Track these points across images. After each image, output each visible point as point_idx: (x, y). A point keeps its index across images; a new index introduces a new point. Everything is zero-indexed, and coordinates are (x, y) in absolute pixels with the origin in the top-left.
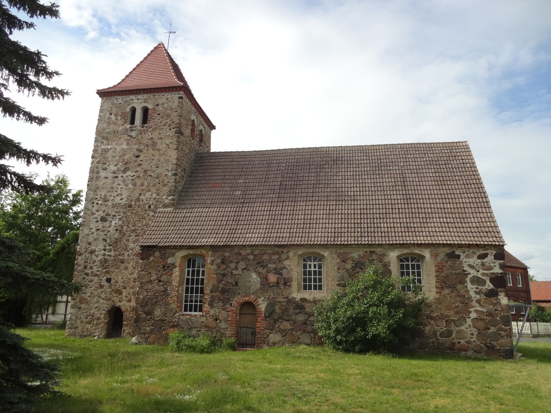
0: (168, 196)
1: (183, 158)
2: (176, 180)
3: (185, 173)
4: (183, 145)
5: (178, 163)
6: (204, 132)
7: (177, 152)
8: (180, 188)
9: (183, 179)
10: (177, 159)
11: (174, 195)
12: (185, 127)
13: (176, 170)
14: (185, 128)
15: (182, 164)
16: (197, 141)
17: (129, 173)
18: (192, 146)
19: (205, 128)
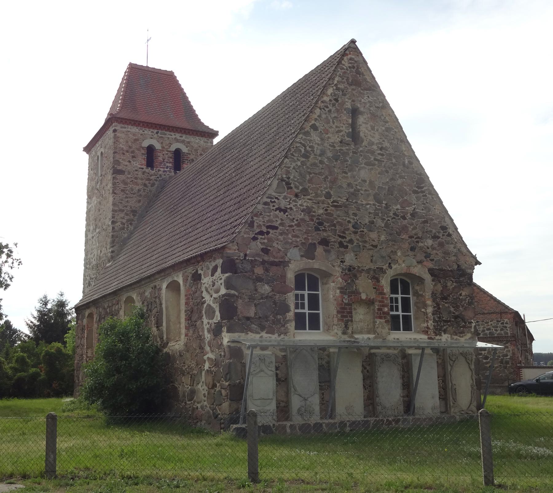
0: (110, 249)
1: (126, 200)
2: (113, 228)
3: (134, 215)
4: (125, 183)
5: (116, 208)
6: (185, 149)
7: (113, 197)
8: (126, 235)
9: (131, 224)
10: (114, 204)
11: (112, 247)
12: (129, 162)
13: (113, 217)
14: (128, 163)
15: (126, 207)
16: (167, 167)
17: (97, 230)
18: (152, 177)
19: (188, 144)
